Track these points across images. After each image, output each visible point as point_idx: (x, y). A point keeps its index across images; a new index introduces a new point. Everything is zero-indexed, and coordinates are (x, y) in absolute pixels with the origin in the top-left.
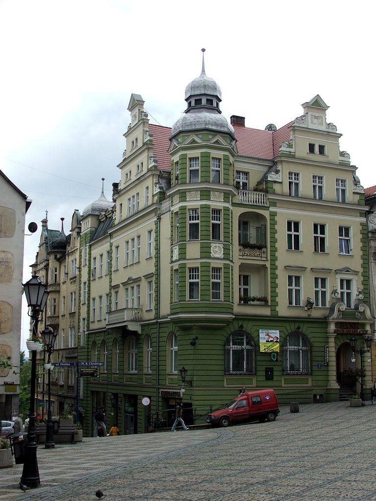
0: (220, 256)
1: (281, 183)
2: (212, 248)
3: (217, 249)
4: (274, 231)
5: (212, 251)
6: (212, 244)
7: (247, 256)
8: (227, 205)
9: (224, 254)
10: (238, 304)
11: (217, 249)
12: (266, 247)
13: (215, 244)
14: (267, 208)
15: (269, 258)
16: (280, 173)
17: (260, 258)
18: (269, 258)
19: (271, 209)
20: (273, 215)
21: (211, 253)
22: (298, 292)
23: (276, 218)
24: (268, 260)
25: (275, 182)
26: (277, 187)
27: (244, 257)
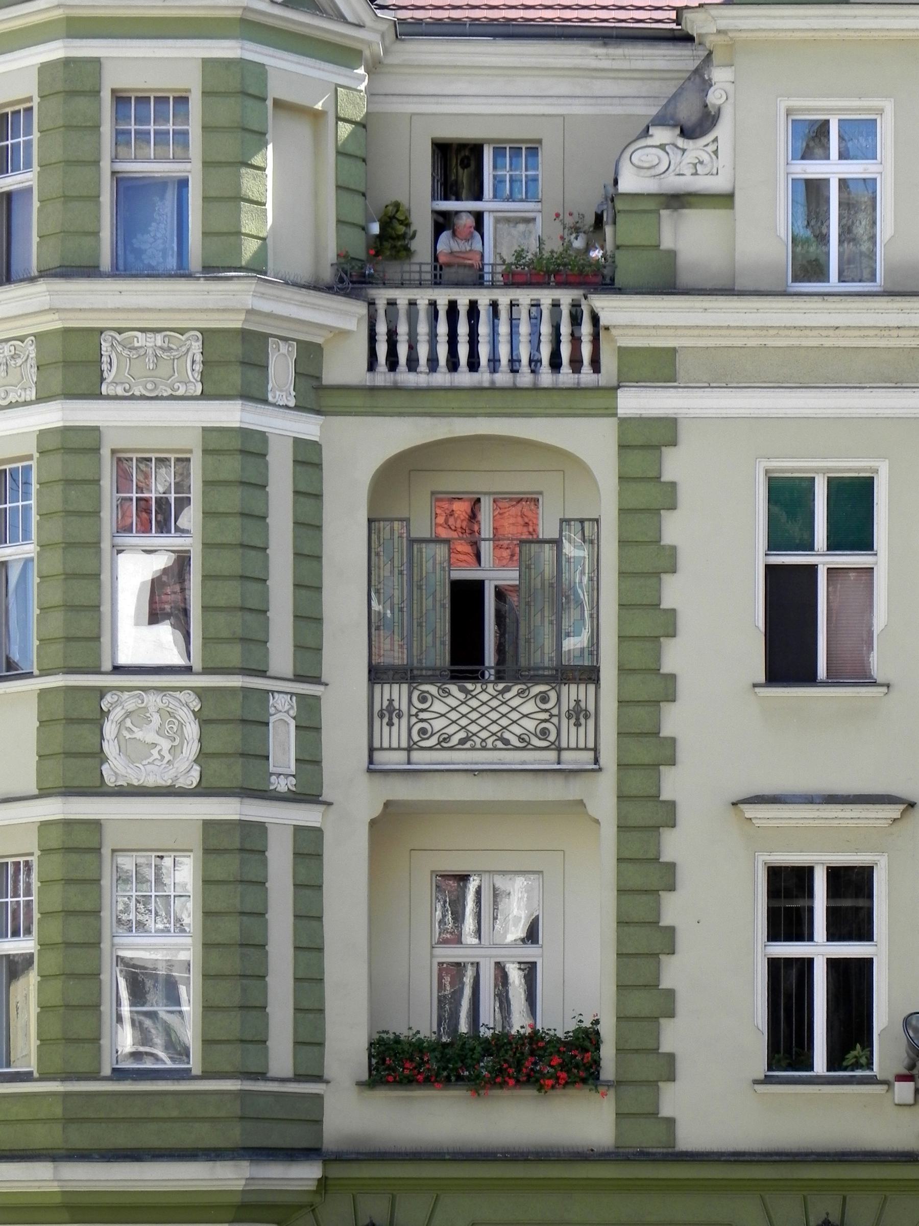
0: (172, 773)
1: (726, 199)
2: (109, 729)
3: (147, 734)
4: (648, 563)
5: (110, 748)
6: (109, 698)
7: (443, 743)
8: (230, 414)
9: (203, 757)
10: (360, 1084)
11: (147, 734)
12: (591, 675)
13: (130, 702)
14: (599, 400)
16: (723, 131)
19: (634, 402)
20: (647, 442)
21: (100, 756)
22: (852, 980)
23: (675, 465)
25: (678, 200)
26: (691, 239)
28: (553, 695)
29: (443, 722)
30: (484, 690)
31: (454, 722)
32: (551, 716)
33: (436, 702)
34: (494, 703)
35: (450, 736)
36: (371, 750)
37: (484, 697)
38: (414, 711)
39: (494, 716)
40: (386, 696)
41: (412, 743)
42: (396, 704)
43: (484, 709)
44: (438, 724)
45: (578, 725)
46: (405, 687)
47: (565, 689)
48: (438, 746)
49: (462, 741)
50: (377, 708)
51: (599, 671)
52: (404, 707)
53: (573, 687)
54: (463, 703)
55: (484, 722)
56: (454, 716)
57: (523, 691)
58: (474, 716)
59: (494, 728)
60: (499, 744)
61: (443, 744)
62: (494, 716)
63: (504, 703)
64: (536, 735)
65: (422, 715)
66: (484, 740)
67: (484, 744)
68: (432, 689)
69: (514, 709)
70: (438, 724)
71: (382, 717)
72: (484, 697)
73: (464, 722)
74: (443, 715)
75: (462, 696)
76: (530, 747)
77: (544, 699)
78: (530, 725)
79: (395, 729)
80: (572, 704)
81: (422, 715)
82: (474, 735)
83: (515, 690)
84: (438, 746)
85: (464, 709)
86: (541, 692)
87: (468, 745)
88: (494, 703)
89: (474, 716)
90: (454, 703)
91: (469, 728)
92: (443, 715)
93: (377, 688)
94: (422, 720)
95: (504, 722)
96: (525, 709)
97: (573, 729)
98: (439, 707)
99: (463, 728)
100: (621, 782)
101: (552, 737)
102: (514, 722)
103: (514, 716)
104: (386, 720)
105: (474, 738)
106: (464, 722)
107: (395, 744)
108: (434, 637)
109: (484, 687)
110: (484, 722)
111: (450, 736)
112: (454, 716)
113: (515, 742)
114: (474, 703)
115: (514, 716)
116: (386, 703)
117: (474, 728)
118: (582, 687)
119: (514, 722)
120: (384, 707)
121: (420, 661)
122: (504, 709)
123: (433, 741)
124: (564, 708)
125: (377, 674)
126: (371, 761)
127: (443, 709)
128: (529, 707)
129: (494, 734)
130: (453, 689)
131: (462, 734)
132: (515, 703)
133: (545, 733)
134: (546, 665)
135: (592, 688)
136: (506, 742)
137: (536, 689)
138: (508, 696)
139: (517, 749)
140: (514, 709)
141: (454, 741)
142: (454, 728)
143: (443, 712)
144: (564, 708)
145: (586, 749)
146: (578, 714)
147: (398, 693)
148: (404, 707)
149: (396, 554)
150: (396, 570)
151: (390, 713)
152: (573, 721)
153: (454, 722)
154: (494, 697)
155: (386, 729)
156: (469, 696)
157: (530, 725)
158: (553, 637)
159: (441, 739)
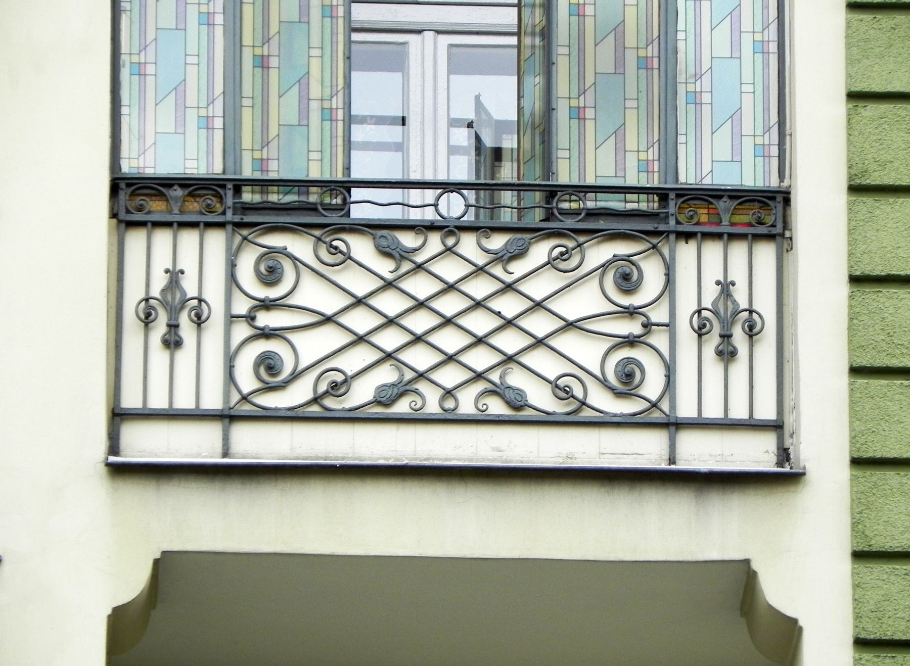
12: (762, 214)
15: (824, 443)
17: (644, 449)
18: (824, 443)
24: (784, 477)
27: (256, 443)
28: (652, 273)
29: (327, 340)
30: (449, 250)
31: (360, 339)
32: (648, 326)
33: (308, 280)
34: (480, 288)
35: (348, 381)
36: (118, 416)
37: (450, 270)
38: (242, 306)
39: (480, 323)
40: (162, 261)
41: (235, 397)
42: (190, 286)
43: (450, 305)
44: (314, 345)
45: (727, 354)
46: (216, 241)
47: (686, 252)
48: (315, 409)
49: (386, 397)
50: (133, 294)
51: (787, 201)
52: (214, 294)
53: (713, 251)
54: (389, 285)
55: (451, 341)
56: (361, 321)
57: (565, 256)
58: (420, 322)
59: (480, 359)
60: (496, 407)
61: (329, 402)
62: (480, 323)
63: (509, 288)
64: (603, 382)
65: (265, 319)
66: (449, 393)
67: (449, 404)
68: (300, 246)
69: (538, 305)
70: (314, 345)
71: (147, 319)
72: (450, 270)
73: (390, 340)
74: (328, 320)
75: (385, 267)
76: (587, 414)
77: (628, 282)
78: (587, 352)
79: (186, 356)
80: (711, 293)
81: (265, 319)
82: (421, 376)
83: (540, 252)
84: (315, 409)
85: (391, 304)
86: (616, 258)
87: (402, 407)
88: (480, 288)
89: (420, 322)
90: (361, 285)
91: (404, 356)
92: (328, 320)
93: (136, 240)
94: (266, 334)
95: (510, 342)
96: (572, 306)
97: (713, 369)
98: (316, 295)
99: (389, 356)
100: (861, 511)
101: (652, 387)
102: (540, 342)
103: (540, 325)
104: (160, 329)
105: (422, 386)
106: (390, 340)
107: (185, 402)
108: (305, 99)
109: (450, 241)
110: (451, 341)
111: (348, 381)
112: (361, 321)
113: (541, 398)
114: (421, 286)
115: (540, 325)
116: (159, 282)
117: (419, 358)
118: (739, 250)
119: (540, 342)
120: (156, 292)
121: (262, 163)
122: (509, 306)
123: (297, 395)
124: (686, 305)
125: (137, 200)
126: (114, 447)
127: (330, 302)
128: (584, 302)
129: (479, 376)
130: (361, 247)
131: (386, 375)
132: (538, 288)
133: (628, 381)
134: (632, 180)
135: (766, 253)
136: (517, 402)
137: (599, 253)
138: (519, 268)
139: (548, 421)
140: (538, 305)
141: (362, 393)
142: (361, 357)
143: (329, 312)
144: (686, 305)
145: (752, 425)
146: (727, 327)
147: (201, 259)
148: (214, 294)
149: (192, 71)
150: (192, 115)
151: (172, 314)
152: (712, 342)
153: (360, 339)
154: (480, 270)
155: (159, 357)
156: (406, 266)
157: (587, 352)
158: (649, 103)
159: (323, 387)
